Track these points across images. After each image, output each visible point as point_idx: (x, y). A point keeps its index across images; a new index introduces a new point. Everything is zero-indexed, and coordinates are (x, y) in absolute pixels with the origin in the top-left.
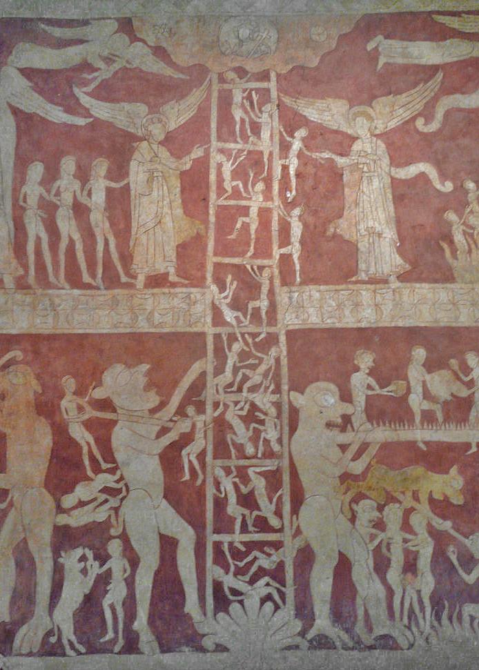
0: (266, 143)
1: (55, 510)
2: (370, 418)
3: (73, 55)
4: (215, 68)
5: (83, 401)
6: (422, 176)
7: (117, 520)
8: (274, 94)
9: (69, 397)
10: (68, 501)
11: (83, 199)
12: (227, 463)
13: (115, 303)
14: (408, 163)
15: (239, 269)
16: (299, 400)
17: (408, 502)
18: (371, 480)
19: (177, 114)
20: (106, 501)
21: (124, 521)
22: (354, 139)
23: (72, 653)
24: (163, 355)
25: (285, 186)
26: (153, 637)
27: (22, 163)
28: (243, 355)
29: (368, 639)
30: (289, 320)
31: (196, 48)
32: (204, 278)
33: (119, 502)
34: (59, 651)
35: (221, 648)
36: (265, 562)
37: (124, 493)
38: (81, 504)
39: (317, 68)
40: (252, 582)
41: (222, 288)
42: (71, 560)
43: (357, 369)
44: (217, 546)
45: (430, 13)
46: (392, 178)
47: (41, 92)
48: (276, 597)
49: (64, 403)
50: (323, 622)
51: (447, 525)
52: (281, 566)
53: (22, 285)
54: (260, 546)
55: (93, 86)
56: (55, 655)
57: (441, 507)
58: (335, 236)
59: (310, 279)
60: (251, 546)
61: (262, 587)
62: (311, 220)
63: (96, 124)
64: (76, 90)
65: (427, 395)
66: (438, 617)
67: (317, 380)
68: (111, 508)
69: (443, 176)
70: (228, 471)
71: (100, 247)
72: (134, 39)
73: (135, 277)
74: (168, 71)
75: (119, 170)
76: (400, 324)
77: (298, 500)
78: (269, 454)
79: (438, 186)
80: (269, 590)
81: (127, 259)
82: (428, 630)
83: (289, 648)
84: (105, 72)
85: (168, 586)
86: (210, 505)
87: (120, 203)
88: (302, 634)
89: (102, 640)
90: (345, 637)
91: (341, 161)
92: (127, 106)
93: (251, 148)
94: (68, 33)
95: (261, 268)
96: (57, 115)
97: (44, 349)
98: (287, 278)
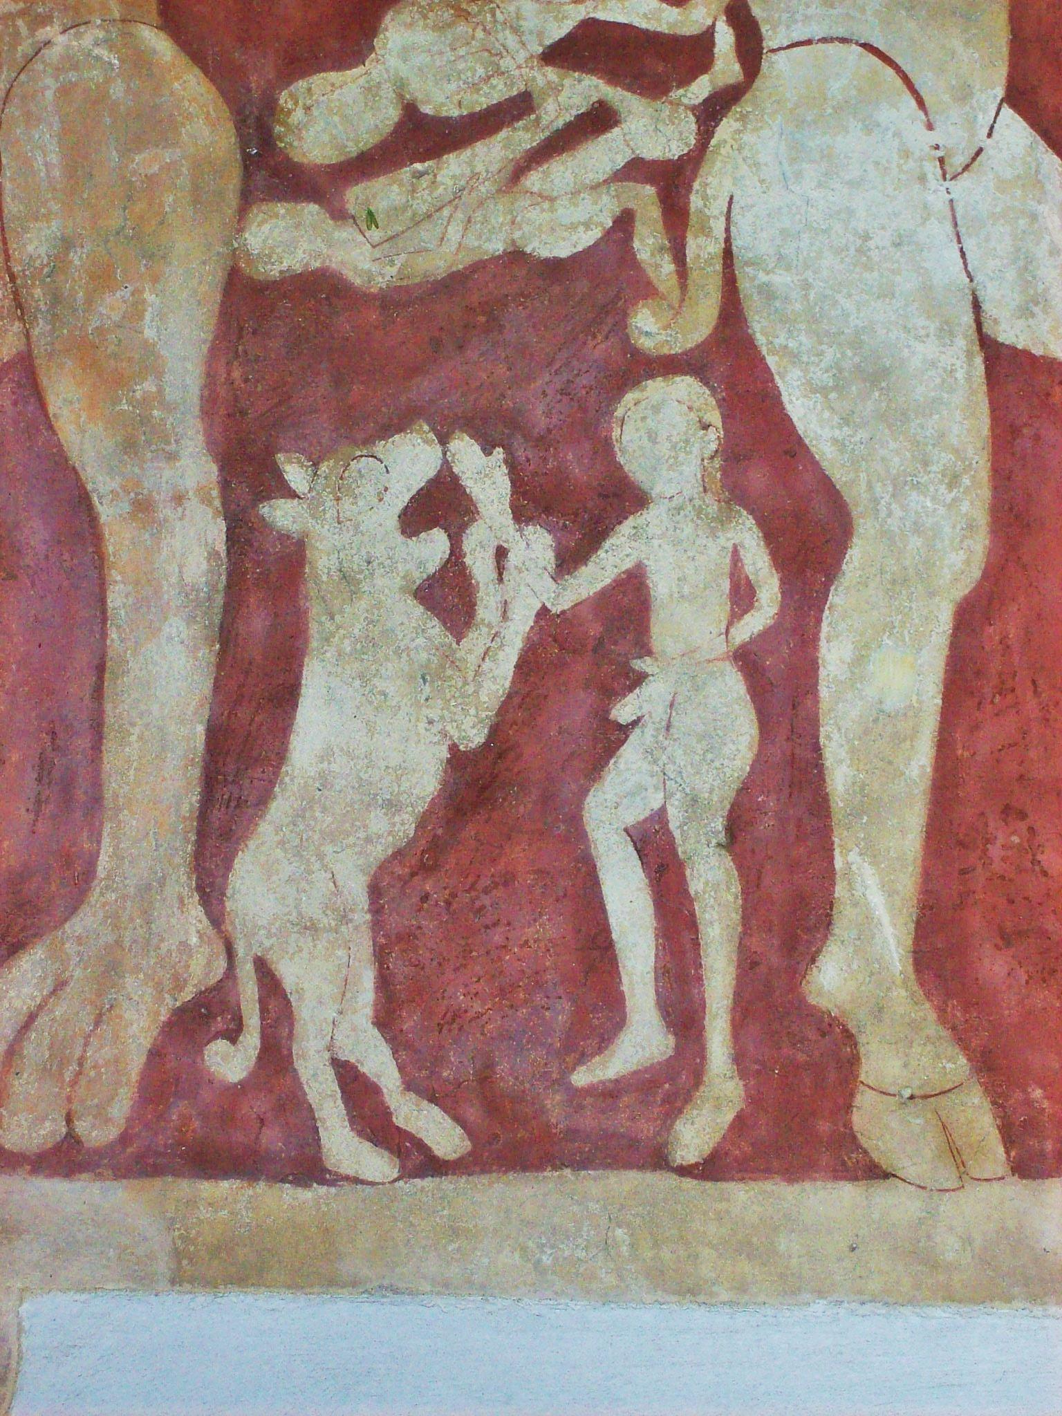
1: (233, 182)
7: (679, 254)
10: (331, 114)
20: (599, 120)
21: (728, 254)
23: (375, 1164)
26: (957, 1065)
33: (689, 126)
34: (272, 1139)
37: (726, 65)
38: (421, 136)
42: (352, 513)
56: (244, 1164)
68: (637, 169)
89: (581, 1078)
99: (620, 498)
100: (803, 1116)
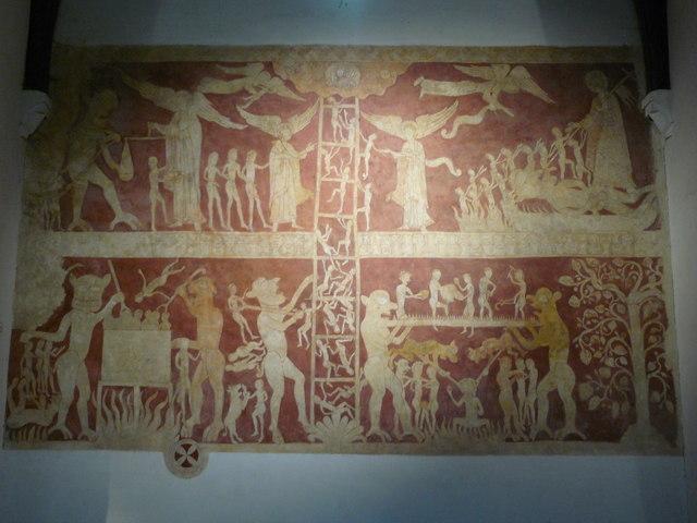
0: (351, 143)
2: (407, 312)
3: (237, 84)
4: (322, 94)
5: (241, 299)
6: (444, 166)
8: (357, 112)
9: (233, 296)
10: (233, 357)
11: (242, 176)
12: (324, 337)
13: (260, 241)
14: (435, 158)
15: (333, 222)
16: (366, 300)
17: (427, 361)
18: (406, 348)
19: (299, 124)
20: (254, 358)
22: (404, 141)
24: (289, 273)
25: (362, 170)
27: (205, 152)
28: (335, 273)
29: (400, 437)
30: (362, 252)
31: (310, 82)
32: (312, 226)
35: (317, 441)
36: (344, 394)
38: (240, 359)
39: (383, 97)
40: (337, 404)
41: (323, 232)
42: (234, 391)
43: (401, 283)
44: (317, 384)
45: (452, 64)
46: (426, 167)
47: (217, 108)
48: (350, 413)
49: (230, 300)
50: (375, 428)
51: (447, 374)
52: (354, 395)
53: (205, 228)
54: (341, 385)
55: (248, 105)
57: (445, 364)
58: (391, 202)
59: (375, 228)
60: (336, 385)
61: (342, 408)
62: (376, 192)
63: (250, 129)
64: (238, 107)
65: (440, 299)
66: (439, 424)
67: (378, 289)
69: (456, 166)
70: (324, 342)
71: (251, 206)
72: (274, 75)
73: (272, 225)
74: (294, 96)
75: (263, 158)
76: (426, 256)
77: (364, 359)
78: (348, 332)
79: (453, 172)
80: (346, 409)
81: (267, 213)
82: (433, 432)
83: (357, 441)
84: (255, 96)
85: (289, 406)
86: (313, 361)
87: (263, 178)
88: (364, 434)
90: (387, 436)
91: (396, 155)
92: (268, 118)
93: (341, 145)
94: (234, 71)
95: (346, 220)
96: (226, 123)
97: (219, 268)
98: (361, 227)
99: (255, 389)
100: (268, 439)
